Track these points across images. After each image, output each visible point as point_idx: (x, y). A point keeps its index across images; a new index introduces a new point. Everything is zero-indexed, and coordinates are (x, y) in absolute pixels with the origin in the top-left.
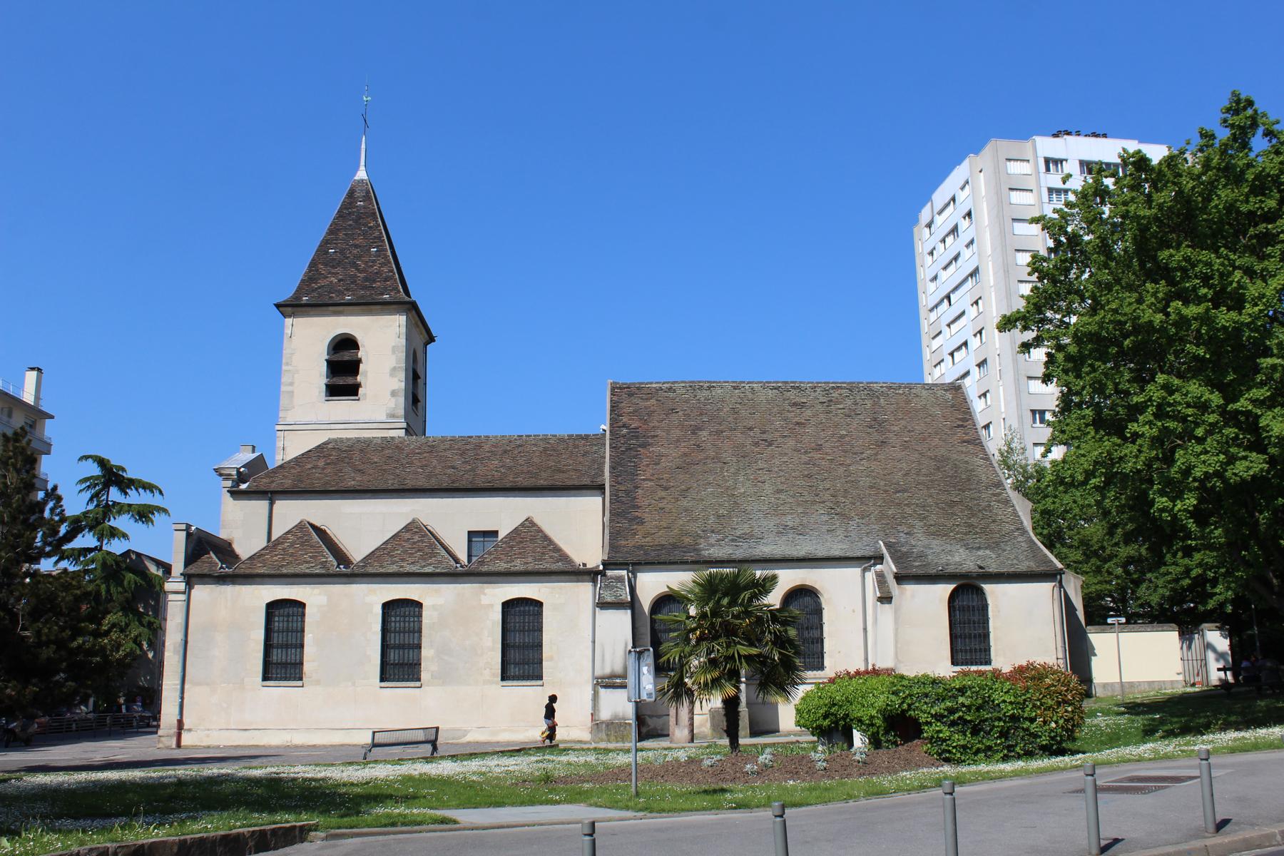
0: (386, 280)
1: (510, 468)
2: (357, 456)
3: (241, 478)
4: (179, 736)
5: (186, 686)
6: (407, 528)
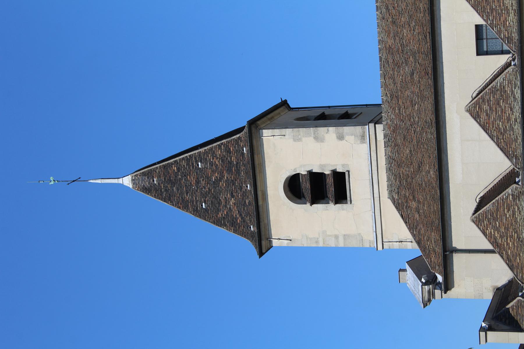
0: (229, 151)
1: (411, 17)
2: (404, 170)
3: (432, 281)
6: (476, 117)
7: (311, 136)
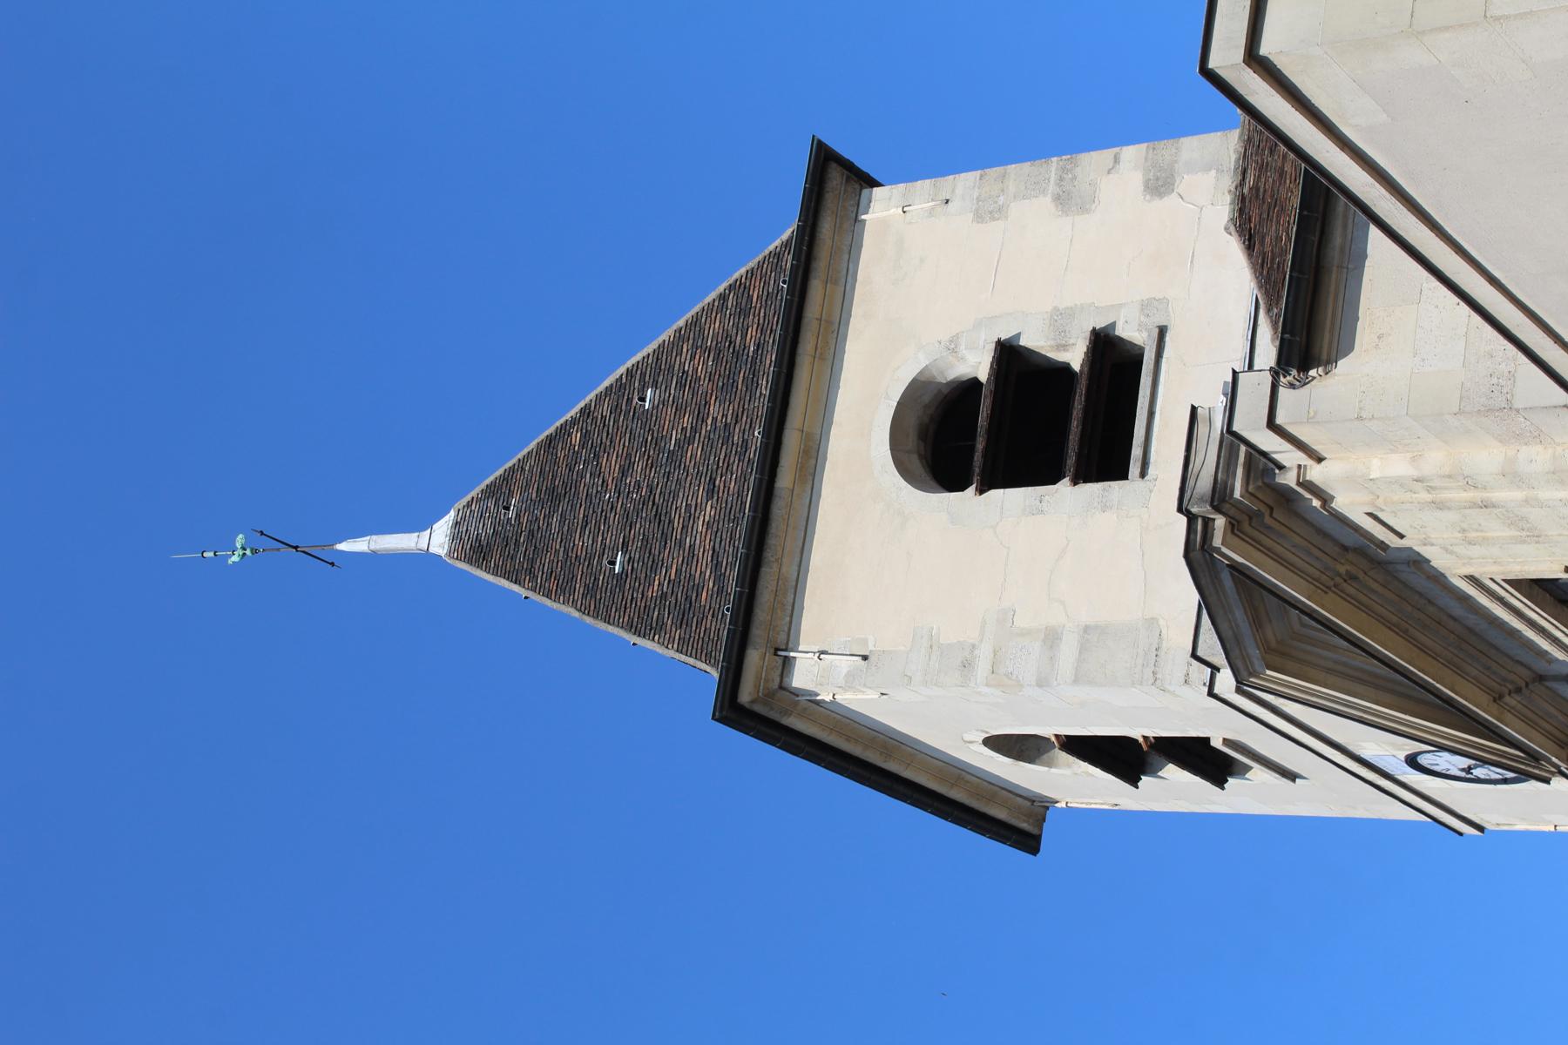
7: (1044, 192)
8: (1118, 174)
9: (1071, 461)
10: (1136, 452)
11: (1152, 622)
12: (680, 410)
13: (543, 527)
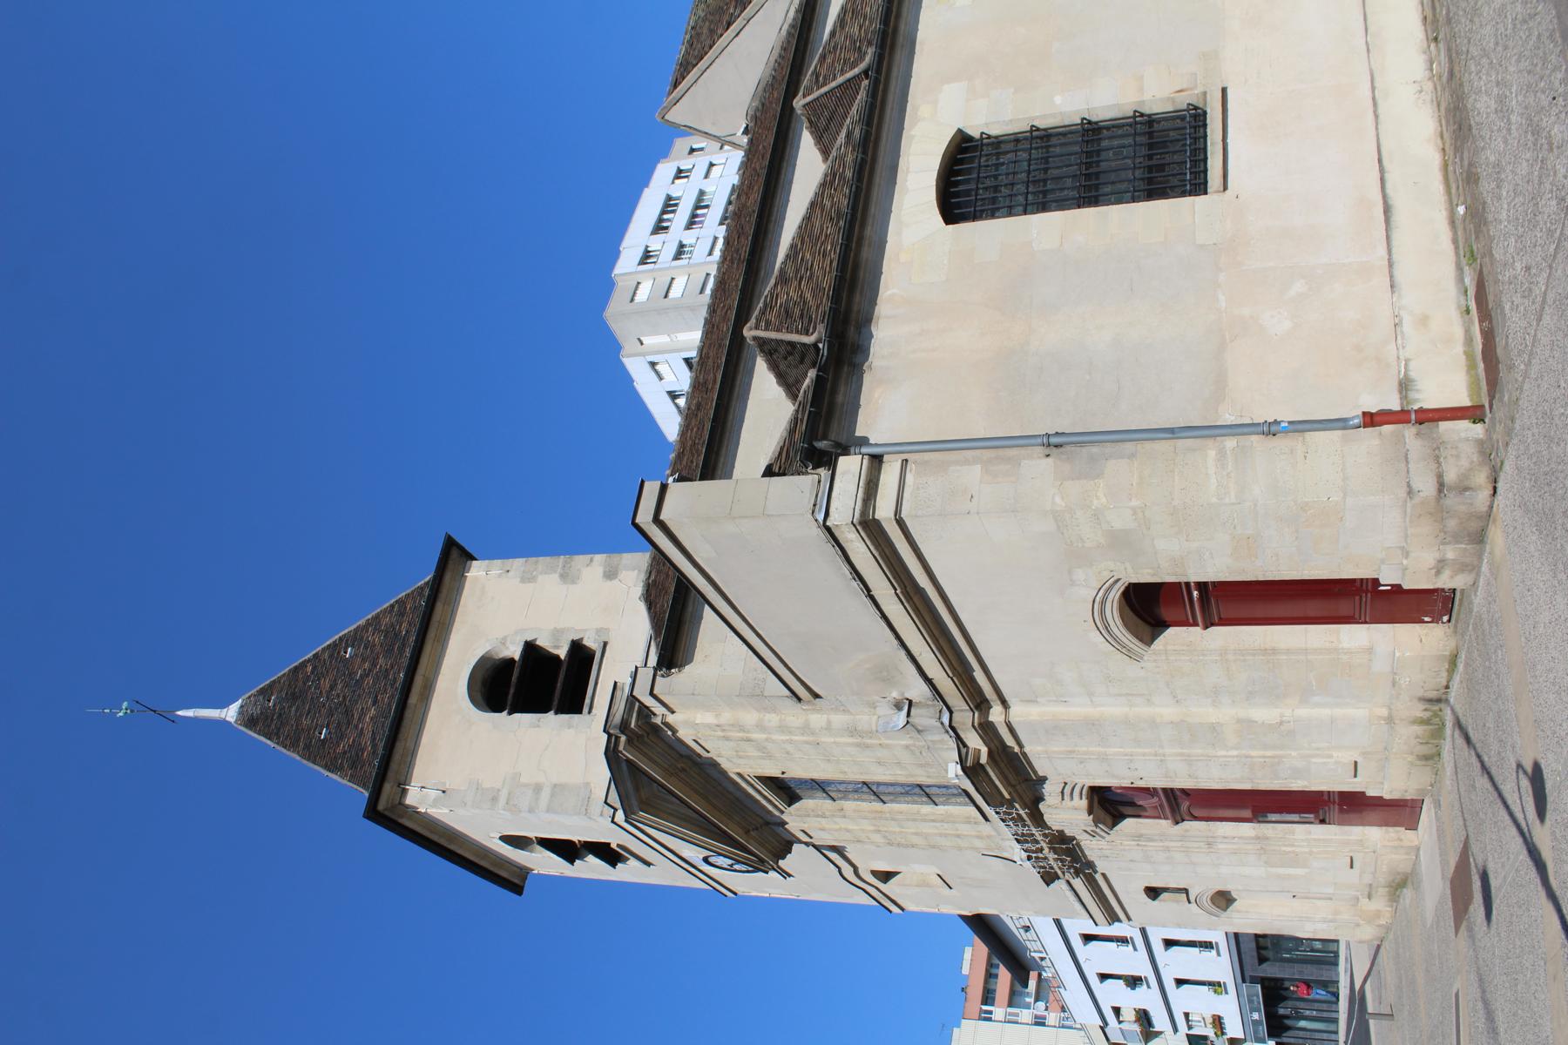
4: (1429, 417)
5: (1229, 418)
8: (591, 568)
9: (555, 703)
10: (587, 701)
11: (587, 784)
12: (364, 660)
13: (285, 713)
